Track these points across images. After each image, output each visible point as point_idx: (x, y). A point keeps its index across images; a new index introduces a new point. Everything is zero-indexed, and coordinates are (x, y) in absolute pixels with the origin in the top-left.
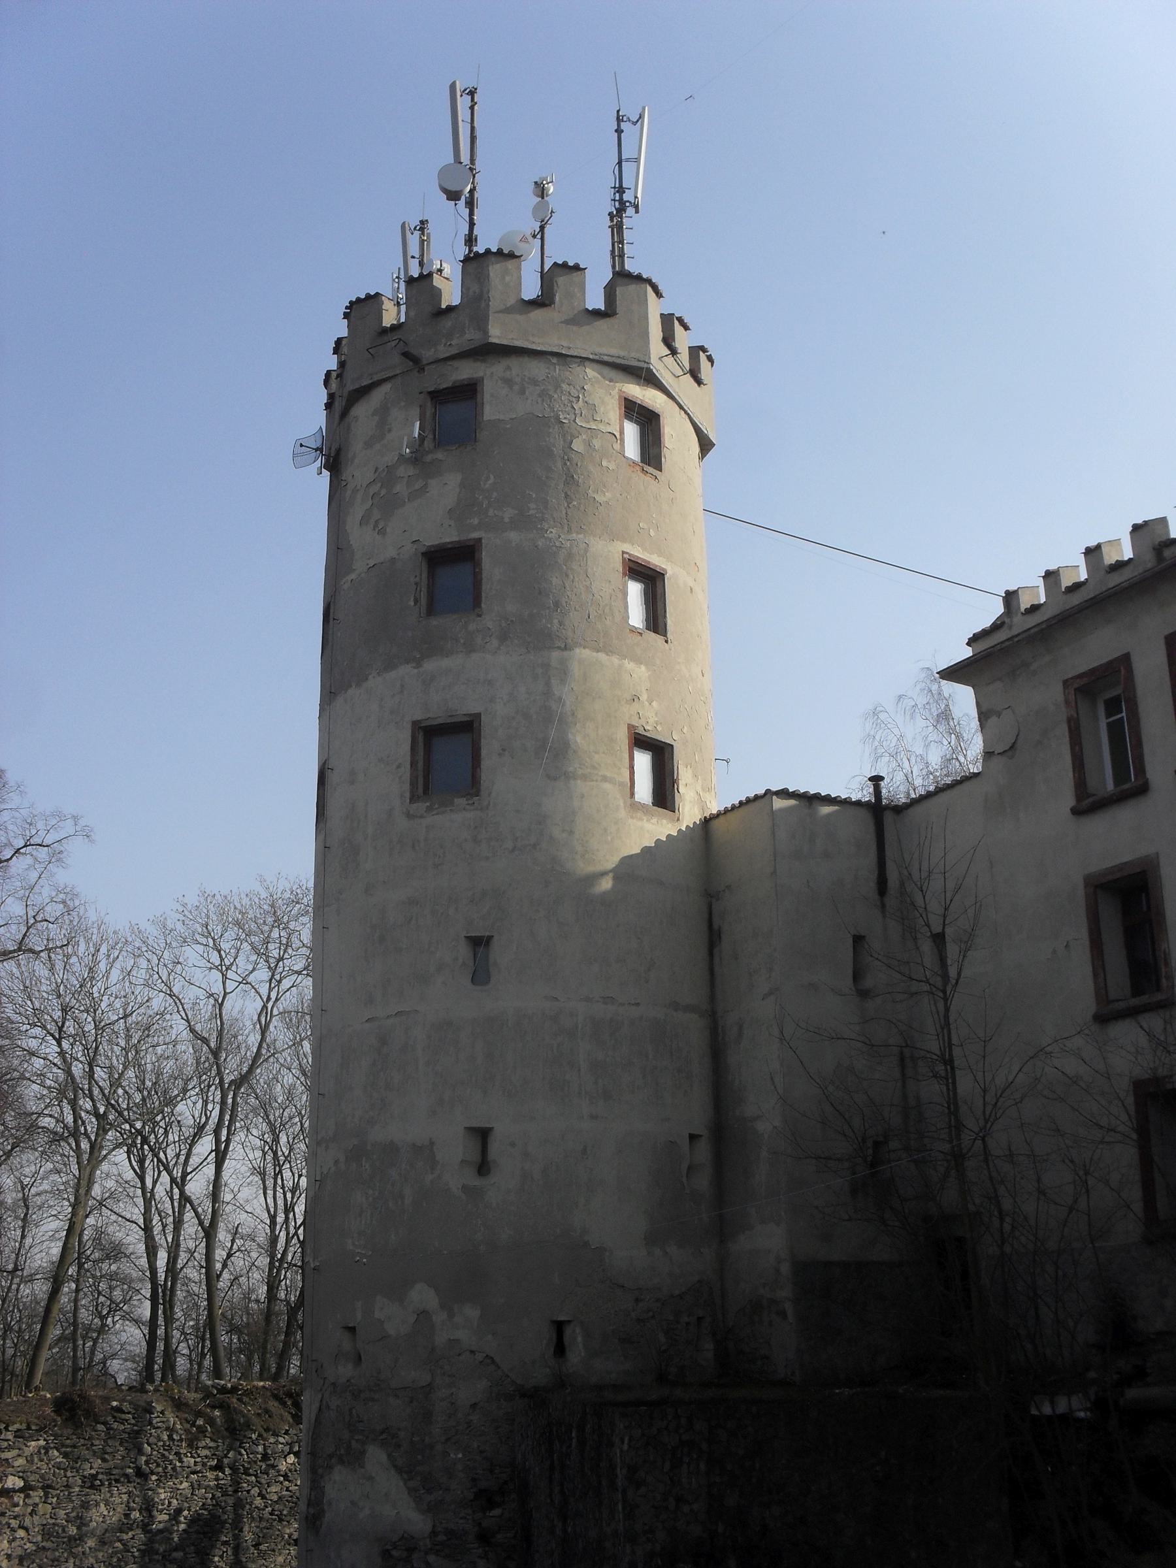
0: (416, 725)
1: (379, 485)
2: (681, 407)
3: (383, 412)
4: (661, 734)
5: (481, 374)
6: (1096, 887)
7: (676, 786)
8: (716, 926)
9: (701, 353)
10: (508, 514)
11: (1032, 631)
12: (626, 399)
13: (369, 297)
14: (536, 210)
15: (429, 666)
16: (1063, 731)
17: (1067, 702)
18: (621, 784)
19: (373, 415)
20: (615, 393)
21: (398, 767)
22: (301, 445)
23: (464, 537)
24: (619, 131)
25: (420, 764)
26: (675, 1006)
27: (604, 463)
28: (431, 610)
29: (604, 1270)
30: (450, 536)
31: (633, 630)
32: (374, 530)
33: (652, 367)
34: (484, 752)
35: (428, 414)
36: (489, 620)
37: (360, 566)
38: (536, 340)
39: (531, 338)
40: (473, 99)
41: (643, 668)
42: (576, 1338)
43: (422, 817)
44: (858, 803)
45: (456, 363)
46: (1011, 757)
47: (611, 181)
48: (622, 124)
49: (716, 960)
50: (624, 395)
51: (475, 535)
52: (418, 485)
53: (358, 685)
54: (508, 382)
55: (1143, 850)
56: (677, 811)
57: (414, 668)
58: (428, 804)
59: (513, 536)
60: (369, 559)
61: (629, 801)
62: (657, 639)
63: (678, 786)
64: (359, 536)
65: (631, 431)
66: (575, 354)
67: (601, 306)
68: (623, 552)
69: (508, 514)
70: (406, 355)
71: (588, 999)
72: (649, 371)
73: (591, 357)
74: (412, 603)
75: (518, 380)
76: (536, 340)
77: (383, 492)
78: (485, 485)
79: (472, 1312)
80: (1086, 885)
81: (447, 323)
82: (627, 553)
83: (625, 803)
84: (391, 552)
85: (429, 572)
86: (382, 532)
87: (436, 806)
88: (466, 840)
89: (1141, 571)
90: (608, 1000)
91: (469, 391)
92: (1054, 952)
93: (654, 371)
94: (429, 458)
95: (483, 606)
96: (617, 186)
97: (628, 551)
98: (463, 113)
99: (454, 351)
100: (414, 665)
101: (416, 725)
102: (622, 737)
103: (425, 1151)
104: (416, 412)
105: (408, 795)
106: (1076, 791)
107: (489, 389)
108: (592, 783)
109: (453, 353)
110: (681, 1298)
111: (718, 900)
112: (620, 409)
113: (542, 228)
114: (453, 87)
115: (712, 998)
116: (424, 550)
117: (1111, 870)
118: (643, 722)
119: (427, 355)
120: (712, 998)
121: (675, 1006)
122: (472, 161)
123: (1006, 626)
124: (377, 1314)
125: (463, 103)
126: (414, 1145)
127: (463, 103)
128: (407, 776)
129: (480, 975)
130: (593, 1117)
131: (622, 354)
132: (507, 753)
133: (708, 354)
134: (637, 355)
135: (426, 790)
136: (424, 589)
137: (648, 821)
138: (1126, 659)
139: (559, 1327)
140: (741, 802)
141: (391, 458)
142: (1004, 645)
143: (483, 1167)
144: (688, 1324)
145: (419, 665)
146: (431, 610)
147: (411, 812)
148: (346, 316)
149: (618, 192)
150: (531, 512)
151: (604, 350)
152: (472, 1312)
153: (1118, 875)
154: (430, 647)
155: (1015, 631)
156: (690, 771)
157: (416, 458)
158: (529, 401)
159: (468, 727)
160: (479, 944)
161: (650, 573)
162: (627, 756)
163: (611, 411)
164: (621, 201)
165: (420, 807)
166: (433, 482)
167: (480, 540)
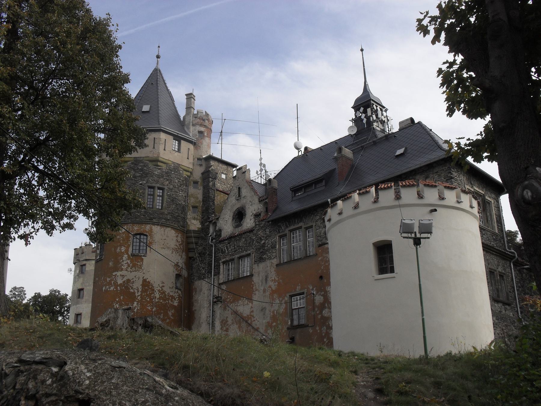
10: (88, 284)
15: (77, 306)
30: (81, 287)
36: (84, 300)
45: (84, 261)
54: (89, 264)
59: (88, 287)
69: (88, 284)
70: (77, 260)
91: (85, 265)
101: (75, 314)
104: (79, 268)
107: (87, 265)
146: (79, 297)
157: (78, 275)
159: (80, 314)
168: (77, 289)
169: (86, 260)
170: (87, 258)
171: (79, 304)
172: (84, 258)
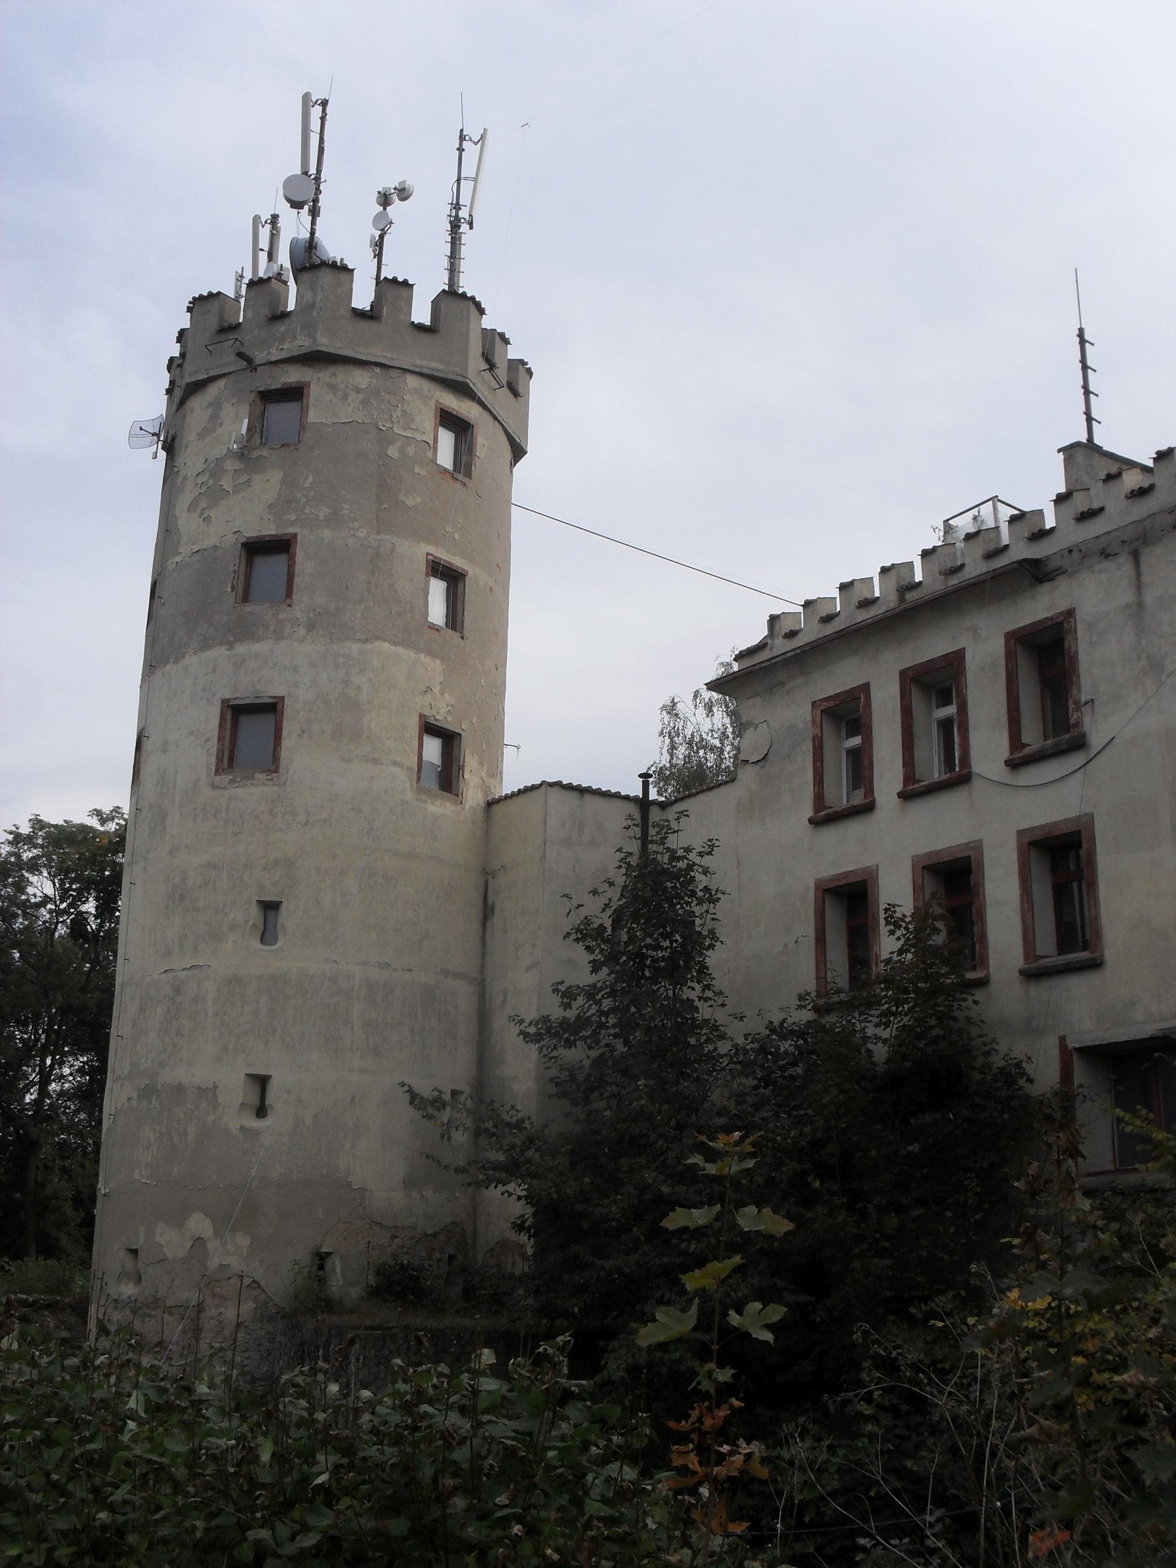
0: (224, 701)
1: (207, 475)
2: (495, 418)
3: (216, 406)
4: (450, 724)
5: (308, 379)
6: (825, 890)
7: (461, 773)
8: (490, 901)
9: (520, 367)
10: (323, 512)
11: (788, 655)
12: (442, 410)
13: (211, 295)
14: (378, 218)
15: (241, 649)
16: (808, 747)
17: (813, 721)
18: (409, 768)
19: (208, 407)
20: (432, 404)
21: (207, 740)
22: (141, 429)
23: (282, 532)
24: (461, 150)
25: (227, 739)
26: (446, 973)
27: (417, 470)
28: (245, 598)
29: (364, 1208)
30: (269, 530)
31: (433, 627)
32: (200, 517)
33: (468, 381)
34: (285, 733)
35: (258, 410)
37: (186, 549)
38: (362, 350)
39: (357, 349)
40: (324, 111)
41: (438, 662)
42: (336, 1265)
43: (224, 788)
44: (627, 798)
45: (285, 367)
46: (763, 767)
47: (449, 197)
48: (464, 142)
49: (488, 932)
50: (441, 406)
51: (292, 530)
52: (244, 478)
53: (176, 662)
54: (333, 388)
55: (866, 862)
56: (460, 795)
57: (226, 649)
58: (231, 777)
59: (327, 533)
60: (194, 544)
61: (415, 785)
62: (456, 635)
63: (463, 772)
64: (187, 523)
65: (446, 440)
66: (398, 365)
67: (426, 320)
68: (428, 554)
69: (323, 512)
70: (240, 355)
71: (364, 963)
72: (467, 385)
73: (412, 369)
74: (230, 590)
75: (342, 386)
76: (362, 350)
77: (211, 482)
78: (304, 483)
79: (243, 1241)
80: (816, 889)
81: (281, 328)
82: (432, 555)
83: (411, 786)
84: (213, 540)
85: (247, 561)
86: (207, 520)
87: (239, 779)
88: (263, 813)
89: (885, 609)
90: (384, 966)
91: (295, 393)
92: (785, 946)
93: (471, 385)
94: (255, 454)
95: (294, 597)
96: (454, 202)
97: (432, 553)
98: (315, 125)
99: (284, 355)
100: (228, 647)
101: (224, 701)
102: (414, 724)
103: (209, 1093)
104: (245, 409)
105: (213, 767)
106: (815, 802)
107: (315, 392)
108: (382, 766)
109: (284, 356)
110: (435, 1237)
111: (494, 877)
112: (435, 419)
113: (382, 237)
114: (306, 97)
115: (483, 967)
116: (244, 540)
117: (839, 877)
118: (434, 712)
119: (260, 357)
120: (483, 967)
121: (446, 973)
122: (319, 171)
123: (768, 647)
124: (157, 1240)
125: (316, 112)
126: (199, 1087)
127: (316, 112)
128: (214, 750)
129: (267, 935)
130: (363, 1071)
131: (440, 367)
132: (305, 734)
133: (528, 366)
134: (456, 369)
135: (231, 764)
136: (242, 577)
137: (432, 803)
138: (866, 688)
139: (321, 1258)
140: (519, 790)
141: (219, 451)
142: (763, 665)
143: (261, 1111)
144: (439, 1260)
145: (231, 648)
147: (216, 784)
148: (189, 310)
149: (454, 208)
150: (345, 512)
151: (424, 363)
152: (243, 1241)
153: (843, 882)
154: (242, 632)
155: (775, 653)
156: (476, 758)
157: (242, 455)
158: (351, 408)
159: (271, 708)
160: (270, 908)
161: (453, 573)
162: (417, 743)
163: (426, 419)
164: (457, 217)
165: (226, 778)
166: (257, 479)
167: (295, 535)
168: (231, 539)
169: (316, 359)
170: (325, 343)
171: (259, 639)
172: (292, 347)
